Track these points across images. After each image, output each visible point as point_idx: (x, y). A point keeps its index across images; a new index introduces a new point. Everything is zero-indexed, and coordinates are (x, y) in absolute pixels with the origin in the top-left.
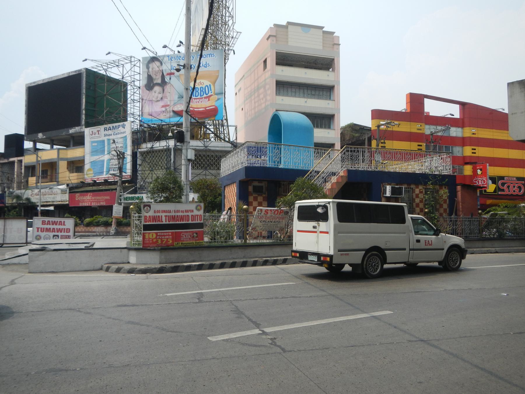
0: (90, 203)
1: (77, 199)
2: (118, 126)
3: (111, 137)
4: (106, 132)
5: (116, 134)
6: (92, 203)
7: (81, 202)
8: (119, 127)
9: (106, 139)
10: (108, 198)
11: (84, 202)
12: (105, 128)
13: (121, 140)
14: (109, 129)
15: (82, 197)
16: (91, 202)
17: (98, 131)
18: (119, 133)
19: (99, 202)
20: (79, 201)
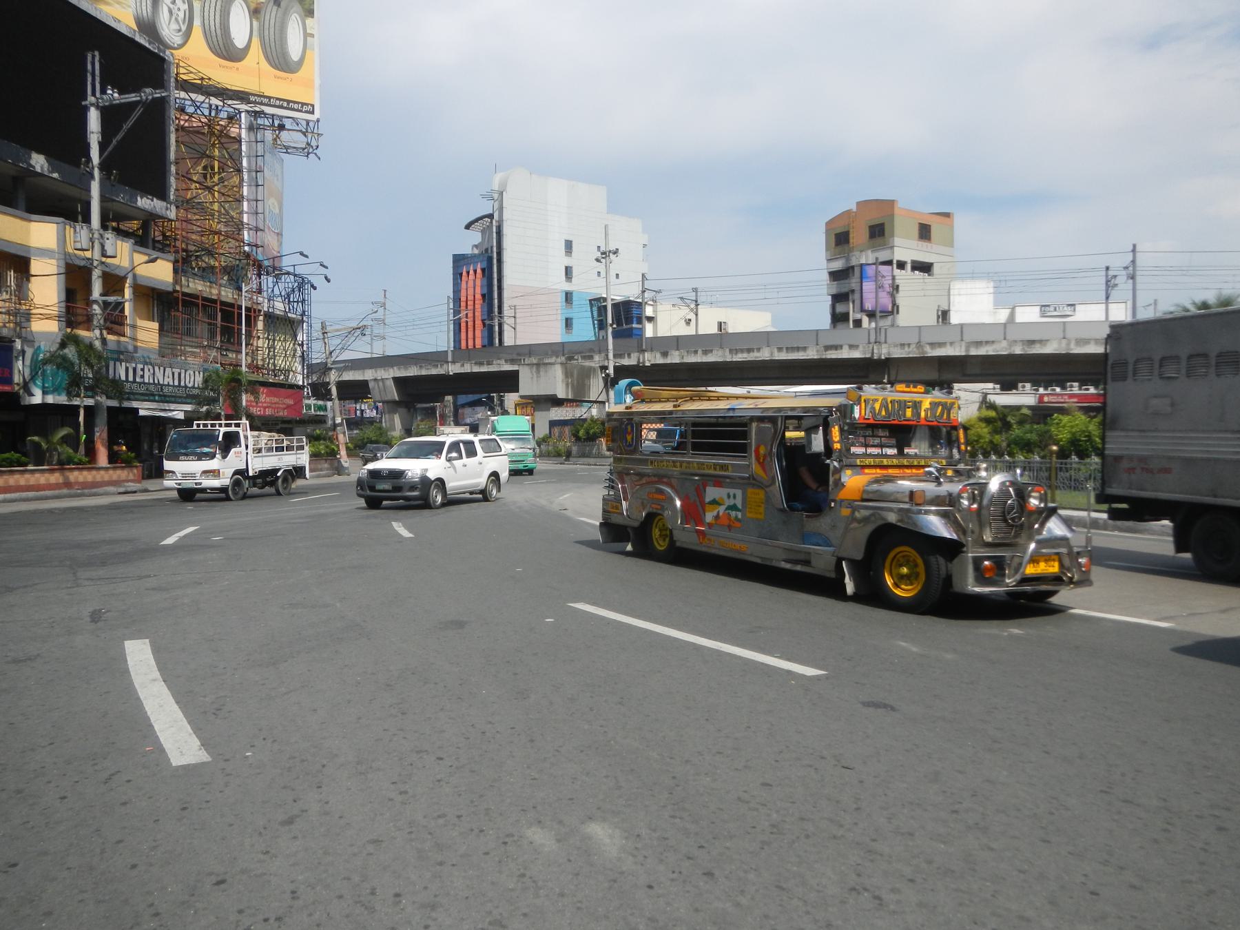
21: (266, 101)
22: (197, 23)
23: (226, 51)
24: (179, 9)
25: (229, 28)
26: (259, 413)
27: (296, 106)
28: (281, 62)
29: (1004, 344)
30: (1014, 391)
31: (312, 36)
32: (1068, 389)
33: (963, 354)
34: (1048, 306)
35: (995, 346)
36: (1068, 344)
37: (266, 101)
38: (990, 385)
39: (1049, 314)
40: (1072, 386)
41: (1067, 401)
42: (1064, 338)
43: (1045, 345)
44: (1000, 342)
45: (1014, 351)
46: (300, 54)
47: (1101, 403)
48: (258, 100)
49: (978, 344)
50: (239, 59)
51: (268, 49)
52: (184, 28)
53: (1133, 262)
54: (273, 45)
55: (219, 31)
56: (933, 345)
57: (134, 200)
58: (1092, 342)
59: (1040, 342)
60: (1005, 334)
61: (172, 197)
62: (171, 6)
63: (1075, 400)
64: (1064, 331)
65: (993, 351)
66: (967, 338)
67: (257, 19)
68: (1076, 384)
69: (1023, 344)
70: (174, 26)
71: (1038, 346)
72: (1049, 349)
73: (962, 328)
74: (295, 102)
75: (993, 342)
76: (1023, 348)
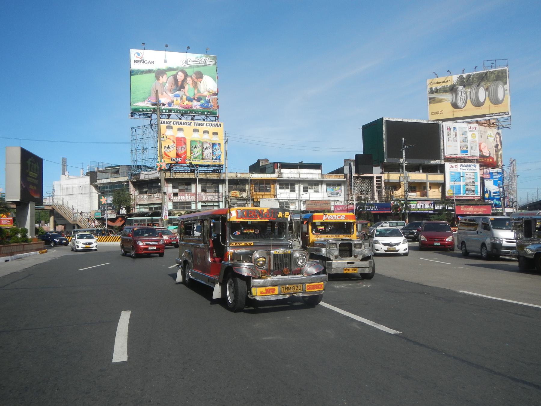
0: (472, 212)
1: (461, 209)
2: (471, 165)
3: (464, 171)
4: (462, 167)
5: (470, 170)
6: (474, 212)
7: (465, 212)
8: (472, 165)
9: (461, 171)
10: (485, 209)
11: (468, 212)
12: (461, 165)
13: (473, 174)
14: (464, 166)
15: (466, 208)
16: (473, 212)
17: (456, 166)
18: (471, 170)
19: (479, 212)
20: (463, 211)
21: (491, 115)
22: (469, 98)
23: (478, 104)
24: (463, 97)
25: (478, 97)
26: (471, 213)
27: (502, 114)
28: (496, 101)
31: (507, 90)
37: (491, 115)
46: (503, 97)
48: (489, 115)
50: (482, 105)
51: (491, 99)
52: (465, 101)
54: (493, 97)
55: (475, 99)
57: (430, 162)
61: (442, 158)
62: (461, 96)
67: (488, 91)
70: (462, 102)
74: (501, 113)
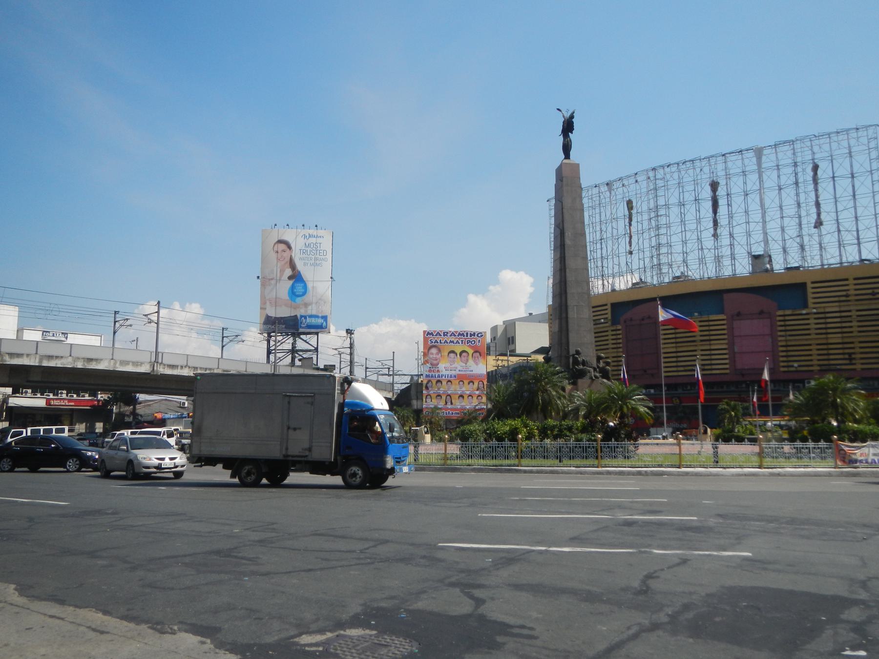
29: (70, 359)
30: (18, 395)
32: (59, 395)
33: (37, 364)
34: (49, 332)
35: (63, 361)
36: (115, 364)
38: (9, 390)
39: (49, 338)
40: (62, 393)
41: (67, 404)
42: (112, 359)
43: (99, 363)
44: (66, 357)
45: (77, 366)
47: (90, 406)
49: (50, 357)
53: (158, 312)
56: (12, 355)
58: (131, 364)
59: (96, 360)
60: (71, 352)
63: (72, 404)
64: (113, 355)
65: (61, 365)
66: (42, 351)
68: (65, 392)
69: (84, 361)
71: (94, 363)
72: (102, 366)
73: (37, 344)
75: (62, 357)
76: (84, 364)
